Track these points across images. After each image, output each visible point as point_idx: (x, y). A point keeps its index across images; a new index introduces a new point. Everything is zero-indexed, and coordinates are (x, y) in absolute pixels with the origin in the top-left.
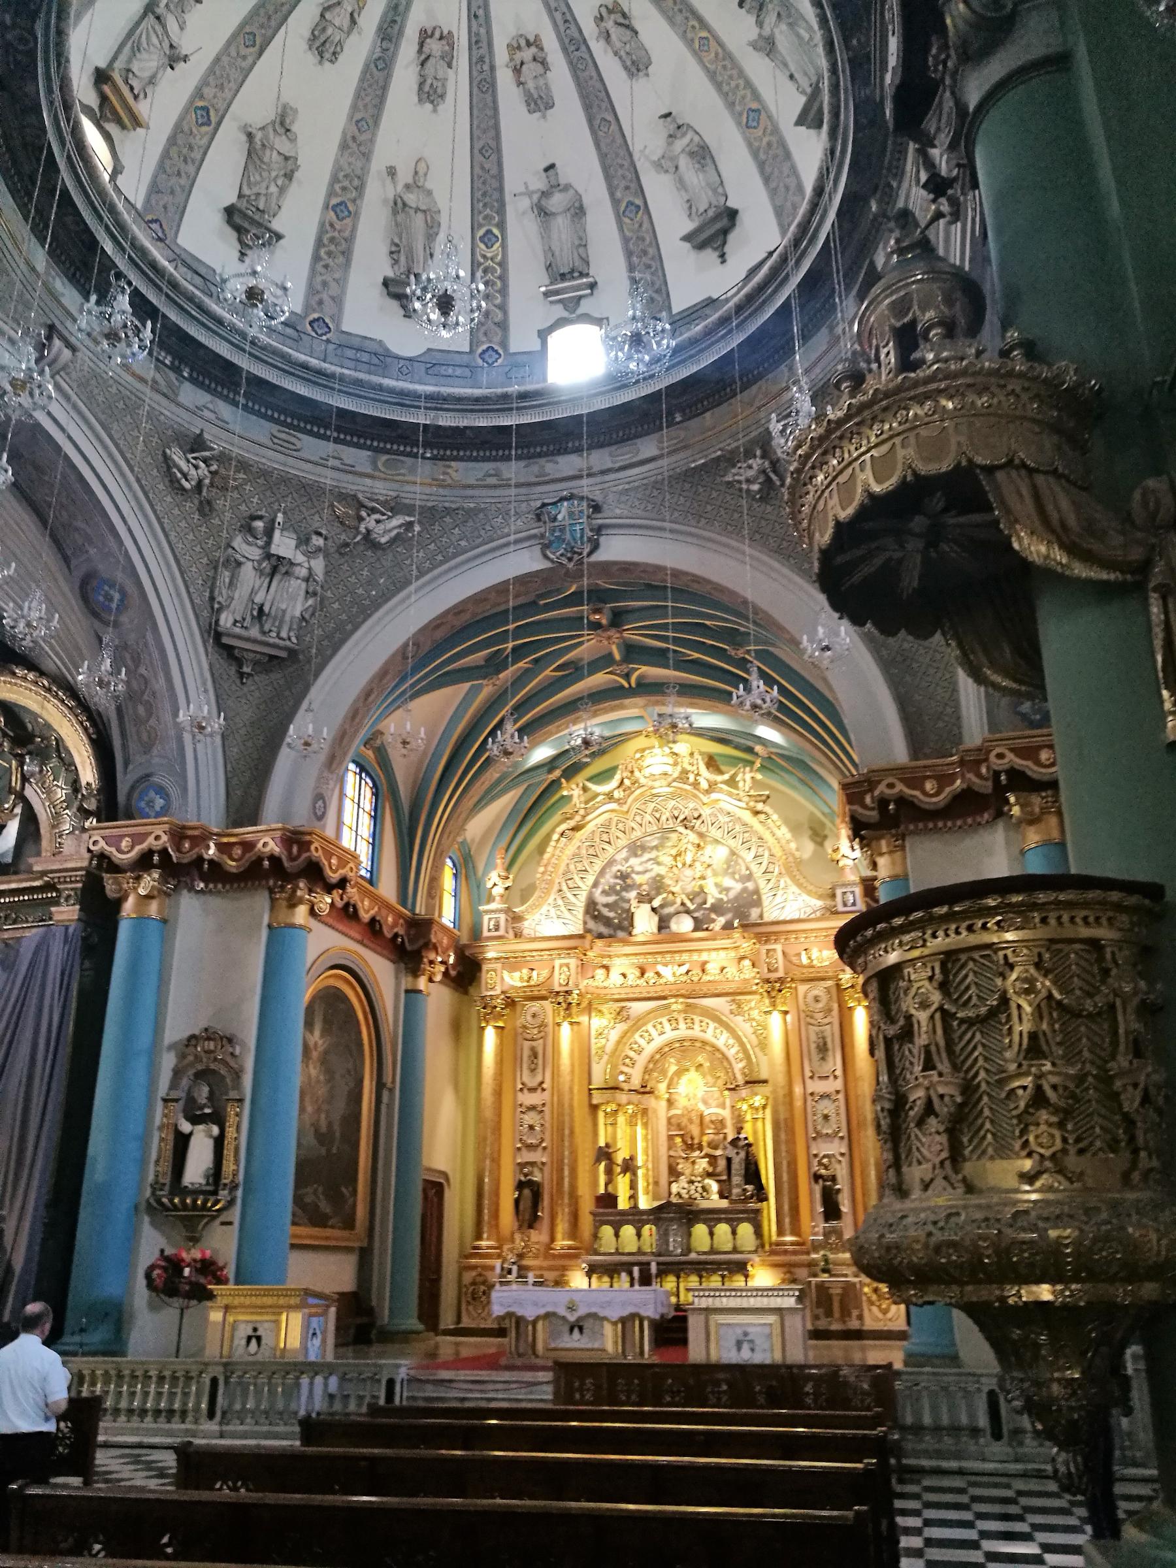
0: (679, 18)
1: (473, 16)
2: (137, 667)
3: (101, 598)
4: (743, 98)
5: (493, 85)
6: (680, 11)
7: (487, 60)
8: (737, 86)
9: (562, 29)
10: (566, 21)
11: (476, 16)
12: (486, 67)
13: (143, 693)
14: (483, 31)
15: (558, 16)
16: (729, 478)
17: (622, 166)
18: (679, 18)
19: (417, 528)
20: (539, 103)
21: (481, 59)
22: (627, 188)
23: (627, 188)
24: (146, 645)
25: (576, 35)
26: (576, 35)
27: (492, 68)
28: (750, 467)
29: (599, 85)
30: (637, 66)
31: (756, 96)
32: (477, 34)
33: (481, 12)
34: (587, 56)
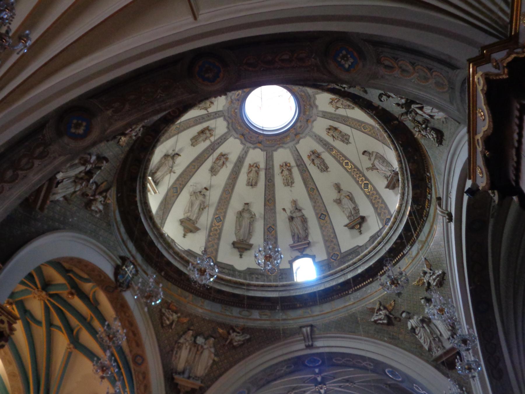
0: (230, 181)
1: (216, 113)
2: (36, 158)
3: (75, 121)
4: (221, 213)
5: (196, 124)
6: (233, 181)
7: (204, 120)
8: (223, 209)
9: (216, 143)
10: (219, 143)
11: (216, 114)
12: (201, 121)
13: (22, 170)
14: (212, 117)
15: (220, 140)
16: (163, 310)
17: (185, 179)
18: (230, 181)
19: (98, 215)
20: (194, 141)
21: (203, 118)
22: (180, 184)
23: (180, 184)
24: (55, 158)
25: (216, 148)
26: (216, 148)
27: (201, 123)
28: (172, 315)
29: (204, 160)
30: (213, 171)
31: (224, 217)
32: (211, 116)
33: (217, 115)
34: (210, 153)
